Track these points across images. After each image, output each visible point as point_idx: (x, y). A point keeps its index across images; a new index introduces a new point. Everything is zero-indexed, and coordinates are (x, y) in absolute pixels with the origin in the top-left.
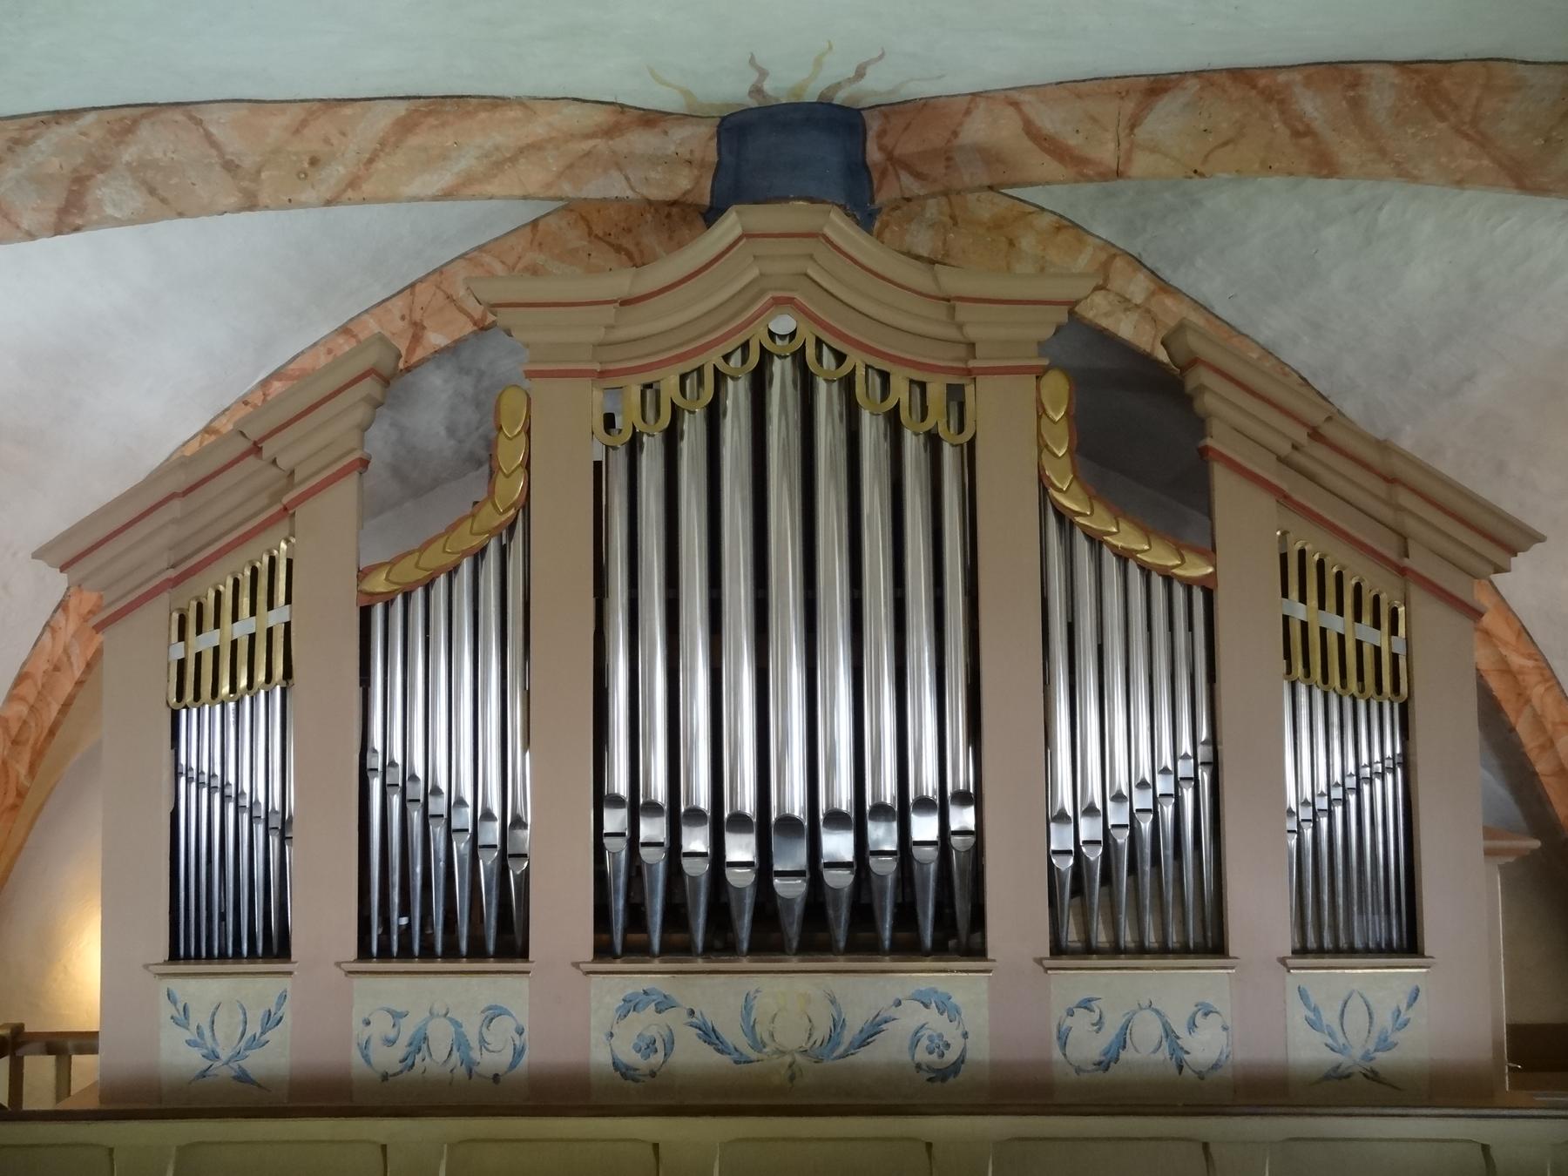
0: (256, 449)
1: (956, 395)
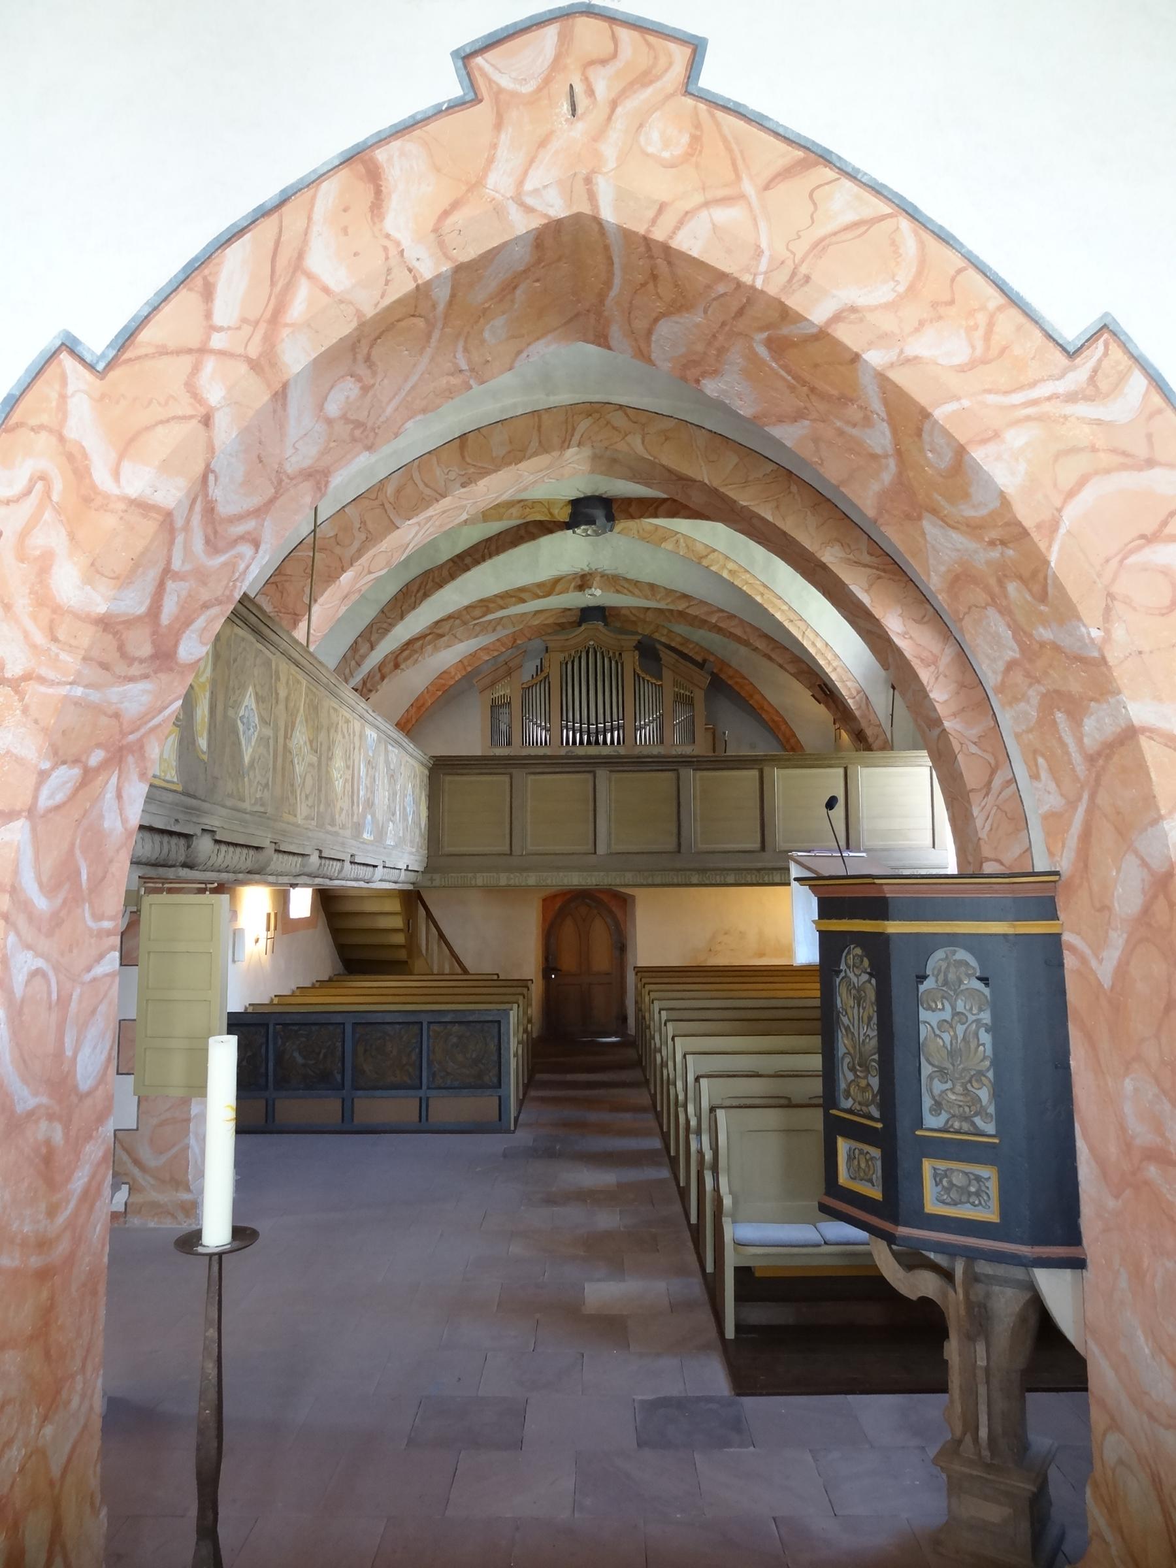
0: (506, 664)
1: (620, 654)
